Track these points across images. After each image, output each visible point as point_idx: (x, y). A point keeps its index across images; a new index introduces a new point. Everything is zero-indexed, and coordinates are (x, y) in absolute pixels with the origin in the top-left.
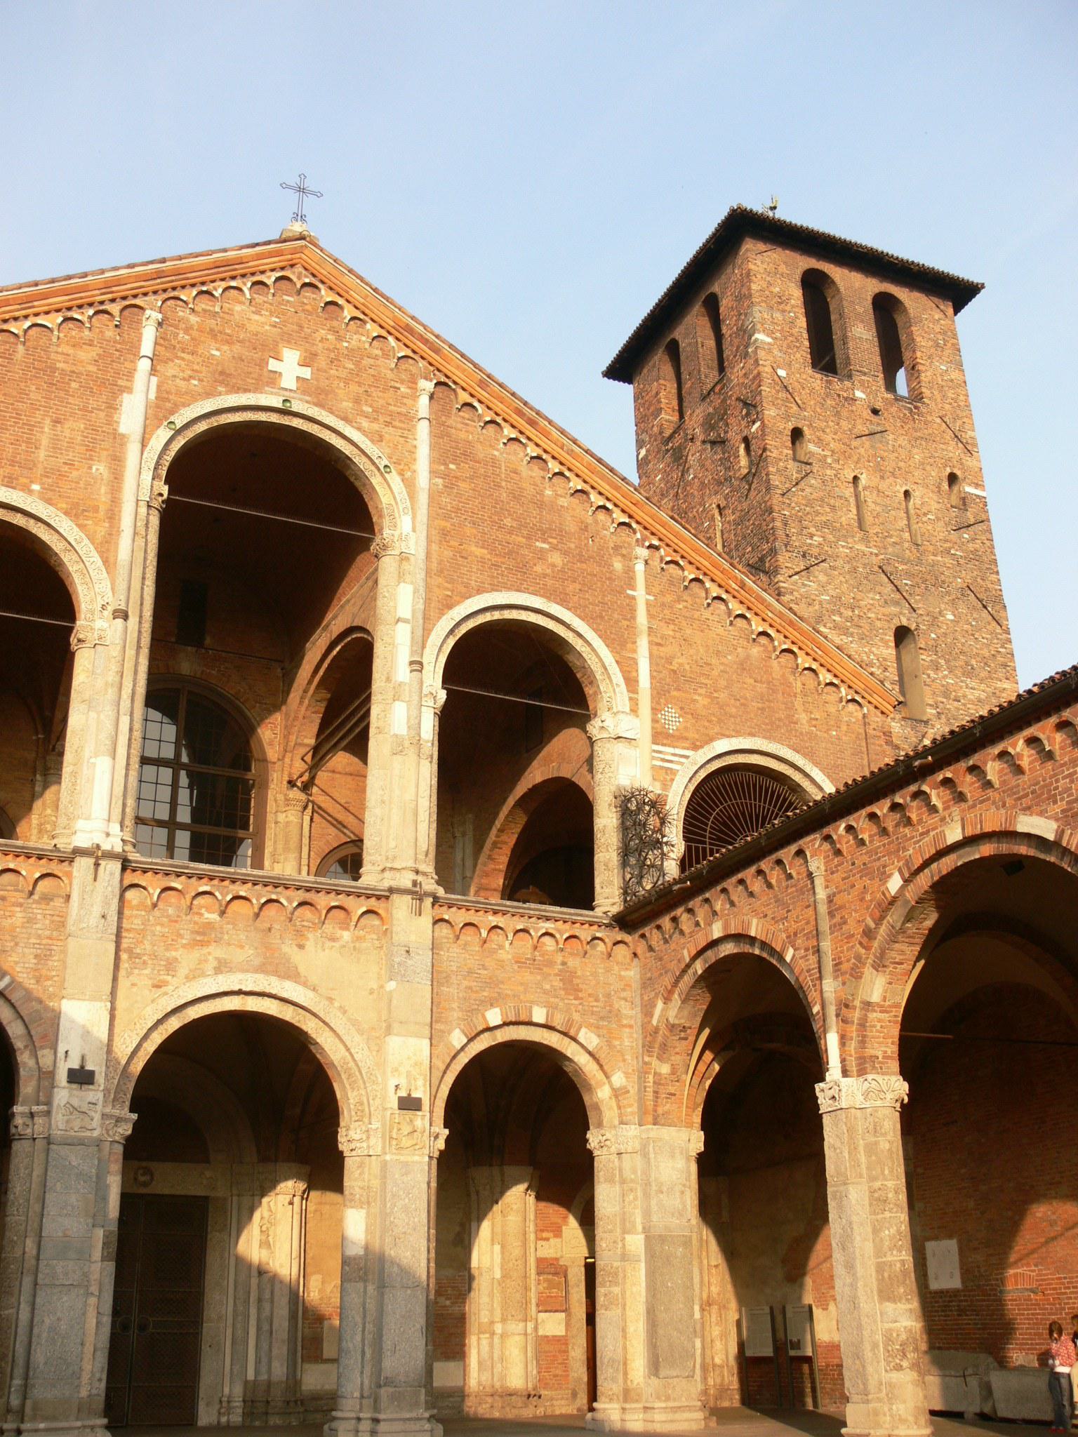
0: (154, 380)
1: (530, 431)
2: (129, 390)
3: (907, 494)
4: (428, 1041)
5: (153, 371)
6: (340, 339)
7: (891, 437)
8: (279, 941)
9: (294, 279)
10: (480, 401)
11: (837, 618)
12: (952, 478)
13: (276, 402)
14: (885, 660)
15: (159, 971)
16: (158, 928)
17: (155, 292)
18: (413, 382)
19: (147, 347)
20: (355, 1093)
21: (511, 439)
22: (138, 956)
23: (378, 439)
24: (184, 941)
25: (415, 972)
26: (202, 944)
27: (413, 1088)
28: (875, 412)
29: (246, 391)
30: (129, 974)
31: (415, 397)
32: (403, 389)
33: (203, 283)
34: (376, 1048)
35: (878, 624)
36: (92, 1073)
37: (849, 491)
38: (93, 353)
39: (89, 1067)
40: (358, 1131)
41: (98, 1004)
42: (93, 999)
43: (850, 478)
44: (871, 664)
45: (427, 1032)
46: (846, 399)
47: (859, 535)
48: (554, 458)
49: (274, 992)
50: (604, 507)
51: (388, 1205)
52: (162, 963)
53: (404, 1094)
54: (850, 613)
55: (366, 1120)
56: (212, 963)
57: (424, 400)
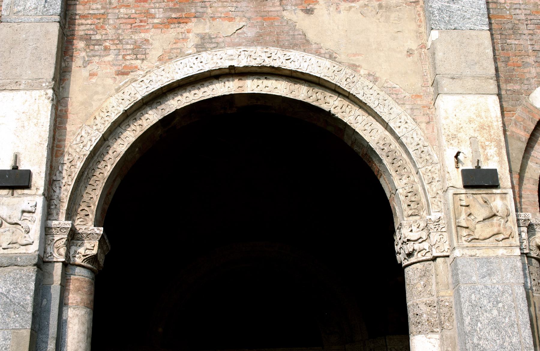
4: (496, 98)
8: (278, 8)
15: (124, 56)
16: (123, 10)
20: (405, 180)
22: (98, 43)
24: (156, 21)
25: (464, 18)
26: (179, 21)
27: (482, 159)
30: (86, 63)
34: (425, 119)
36: (28, 173)
39: (23, 167)
40: (414, 228)
41: (36, 93)
42: (31, 87)
45: (492, 86)
49: (276, 64)
51: (467, 320)
52: (128, 47)
53: (470, 166)
55: (424, 214)
56: (193, 40)
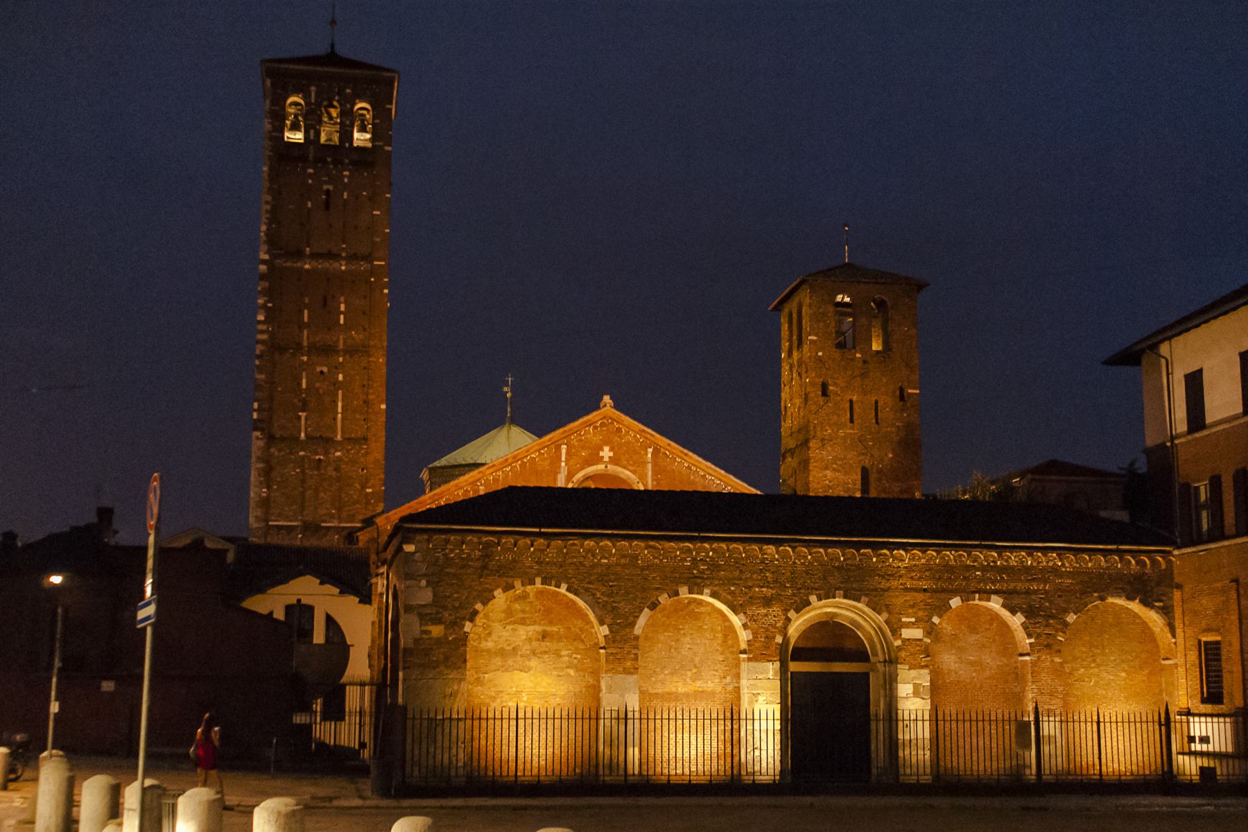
0: (566, 468)
1: (685, 458)
2: (559, 472)
3: (876, 402)
5: (566, 464)
6: (622, 440)
7: (872, 373)
9: (605, 421)
10: (669, 451)
11: (835, 466)
12: (902, 390)
13: (601, 467)
14: (856, 481)
17: (564, 438)
18: (646, 449)
19: (563, 458)
21: (679, 462)
23: (634, 472)
28: (865, 362)
29: (593, 465)
31: (647, 455)
32: (642, 452)
33: (579, 431)
35: (854, 465)
37: (848, 405)
38: (549, 461)
43: (848, 399)
44: (849, 484)
46: (851, 360)
47: (849, 425)
48: (694, 465)
50: (711, 479)
54: (841, 463)
57: (650, 455)
